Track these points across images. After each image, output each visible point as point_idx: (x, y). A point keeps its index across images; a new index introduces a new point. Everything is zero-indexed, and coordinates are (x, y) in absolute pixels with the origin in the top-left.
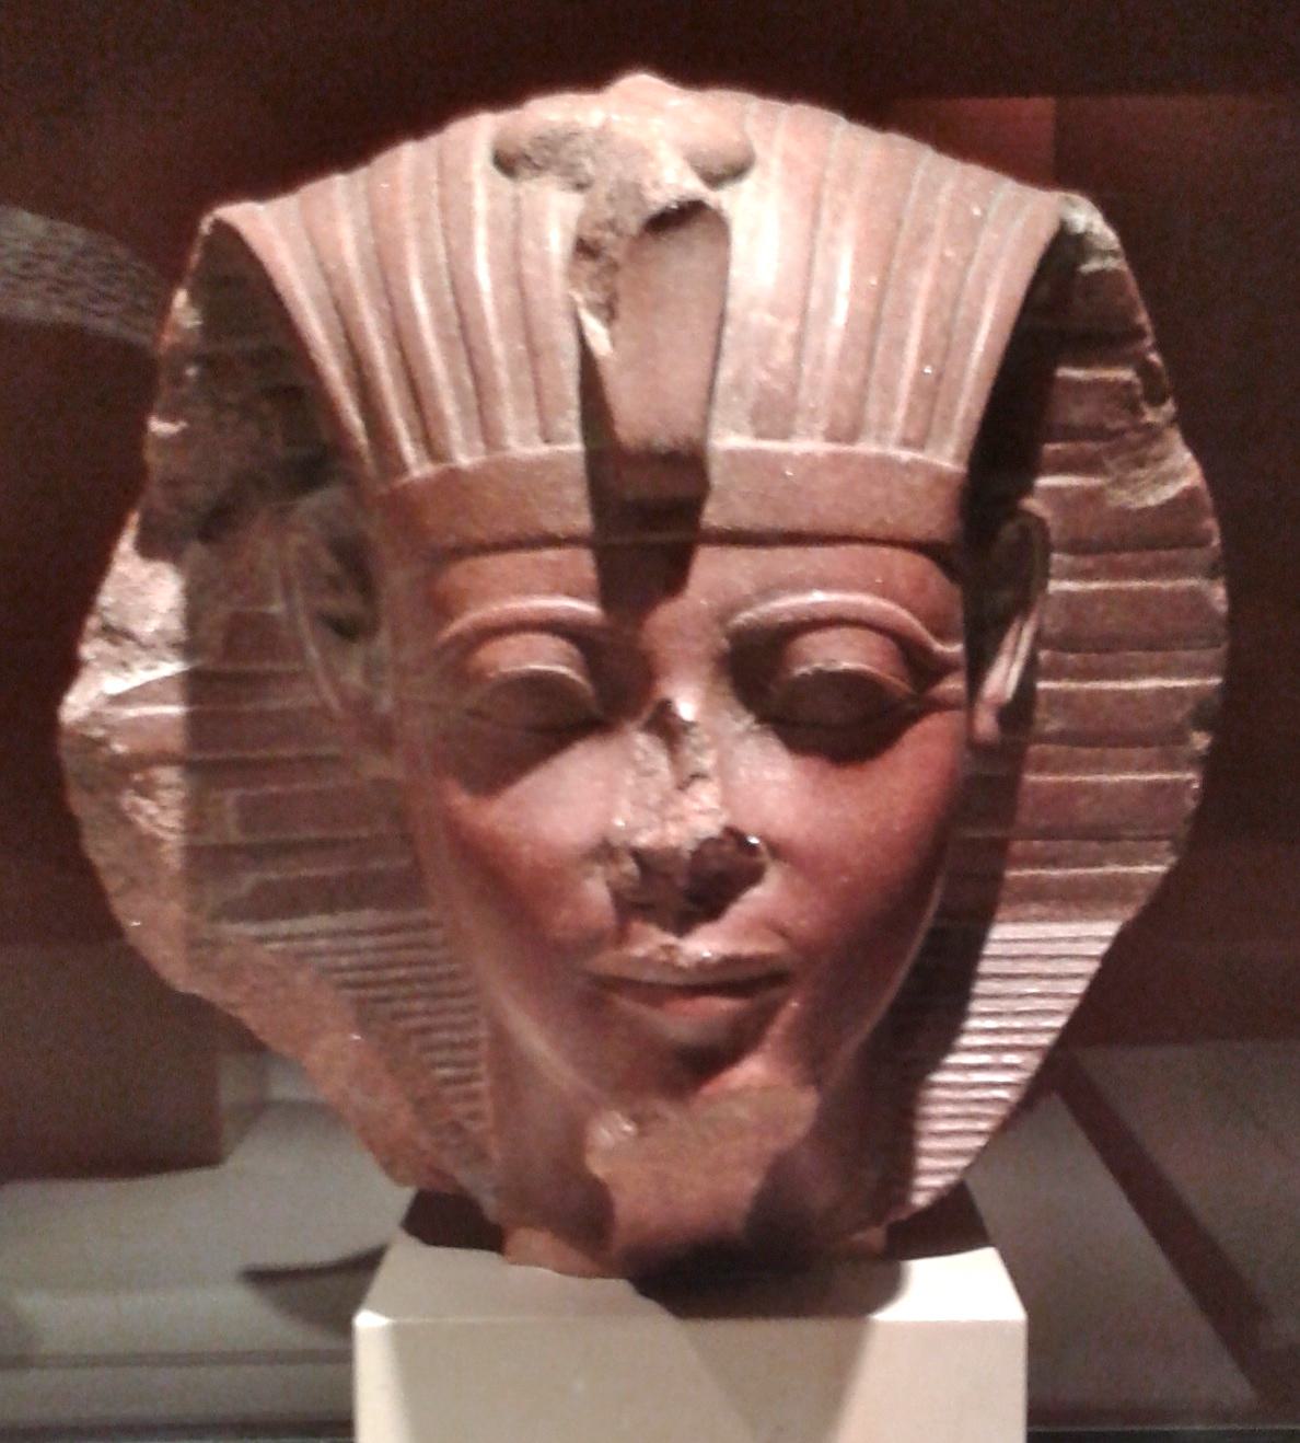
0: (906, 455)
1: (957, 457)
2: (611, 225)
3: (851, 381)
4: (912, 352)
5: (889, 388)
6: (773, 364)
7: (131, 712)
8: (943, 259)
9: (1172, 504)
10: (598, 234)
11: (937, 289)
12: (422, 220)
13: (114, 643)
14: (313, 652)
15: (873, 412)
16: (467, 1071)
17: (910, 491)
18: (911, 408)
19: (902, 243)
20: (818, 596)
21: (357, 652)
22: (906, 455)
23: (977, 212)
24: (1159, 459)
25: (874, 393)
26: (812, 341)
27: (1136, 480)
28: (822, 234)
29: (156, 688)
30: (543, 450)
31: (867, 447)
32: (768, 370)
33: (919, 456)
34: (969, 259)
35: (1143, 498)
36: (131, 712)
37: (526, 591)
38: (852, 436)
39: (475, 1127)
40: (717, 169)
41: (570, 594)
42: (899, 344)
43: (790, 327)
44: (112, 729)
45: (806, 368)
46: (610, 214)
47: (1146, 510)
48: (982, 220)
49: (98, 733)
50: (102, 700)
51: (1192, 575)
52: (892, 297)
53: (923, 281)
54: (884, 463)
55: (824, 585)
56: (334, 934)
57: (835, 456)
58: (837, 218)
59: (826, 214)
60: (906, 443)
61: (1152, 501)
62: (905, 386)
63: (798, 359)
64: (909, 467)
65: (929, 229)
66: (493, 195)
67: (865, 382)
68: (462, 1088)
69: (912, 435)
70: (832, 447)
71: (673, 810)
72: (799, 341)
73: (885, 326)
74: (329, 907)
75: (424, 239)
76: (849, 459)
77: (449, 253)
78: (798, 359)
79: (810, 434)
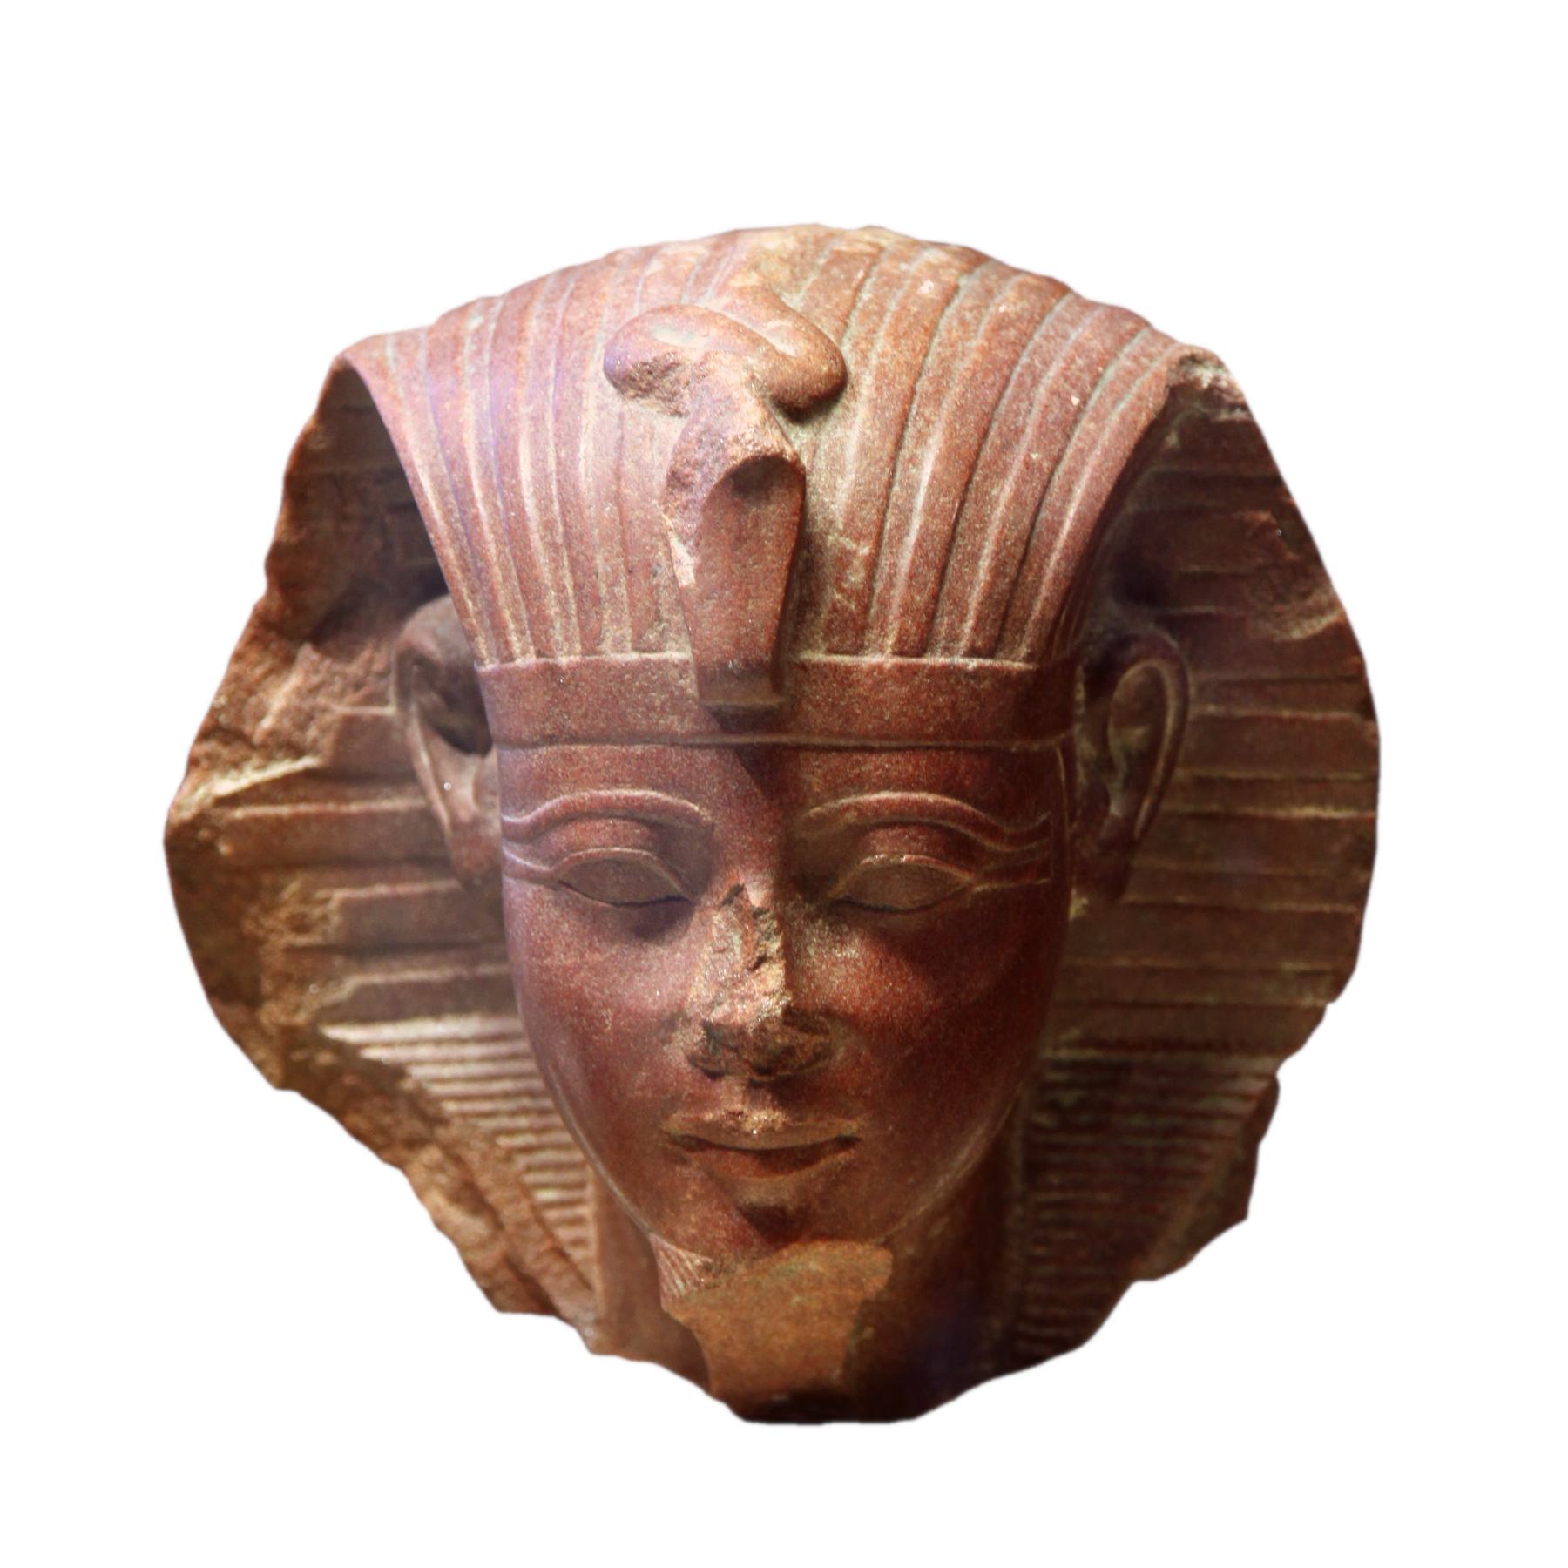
0: (973, 663)
1: (1029, 658)
2: (697, 465)
3: (920, 599)
4: (985, 563)
5: (960, 605)
6: (845, 586)
7: (239, 813)
8: (1028, 464)
9: (1317, 639)
10: (687, 470)
11: (1017, 497)
12: (537, 420)
13: (226, 743)
14: (424, 759)
15: (943, 625)
16: (575, 1194)
17: (975, 695)
18: (980, 620)
19: (987, 451)
20: (884, 795)
21: (472, 764)
22: (973, 663)
23: (1075, 401)
24: (1305, 595)
25: (945, 605)
26: (884, 563)
27: (1279, 615)
28: (905, 454)
29: (263, 790)
30: (634, 657)
31: (935, 659)
32: (841, 590)
33: (988, 662)
34: (1057, 460)
35: (1287, 631)
36: (239, 813)
37: (616, 782)
38: (922, 649)
39: (577, 1254)
40: (801, 402)
41: (655, 787)
42: (975, 557)
43: (865, 550)
44: (217, 832)
45: (879, 586)
46: (699, 456)
47: (1287, 644)
48: (1080, 410)
49: (204, 834)
50: (209, 801)
51: (1340, 708)
52: (969, 512)
53: (1004, 492)
54: (949, 672)
55: (887, 786)
56: (438, 1042)
57: (901, 668)
58: (921, 438)
59: (910, 432)
60: (973, 652)
61: (1300, 632)
62: (974, 599)
63: (871, 577)
64: (977, 674)
65: (1019, 432)
66: (601, 408)
67: (936, 598)
68: (568, 1213)
69: (979, 643)
70: (899, 660)
71: (743, 989)
72: (872, 563)
73: (959, 541)
74: (436, 1012)
75: (535, 442)
76: (915, 670)
77: (559, 463)
78: (871, 577)
79: (881, 650)
